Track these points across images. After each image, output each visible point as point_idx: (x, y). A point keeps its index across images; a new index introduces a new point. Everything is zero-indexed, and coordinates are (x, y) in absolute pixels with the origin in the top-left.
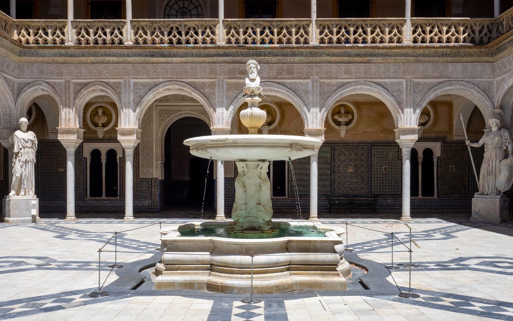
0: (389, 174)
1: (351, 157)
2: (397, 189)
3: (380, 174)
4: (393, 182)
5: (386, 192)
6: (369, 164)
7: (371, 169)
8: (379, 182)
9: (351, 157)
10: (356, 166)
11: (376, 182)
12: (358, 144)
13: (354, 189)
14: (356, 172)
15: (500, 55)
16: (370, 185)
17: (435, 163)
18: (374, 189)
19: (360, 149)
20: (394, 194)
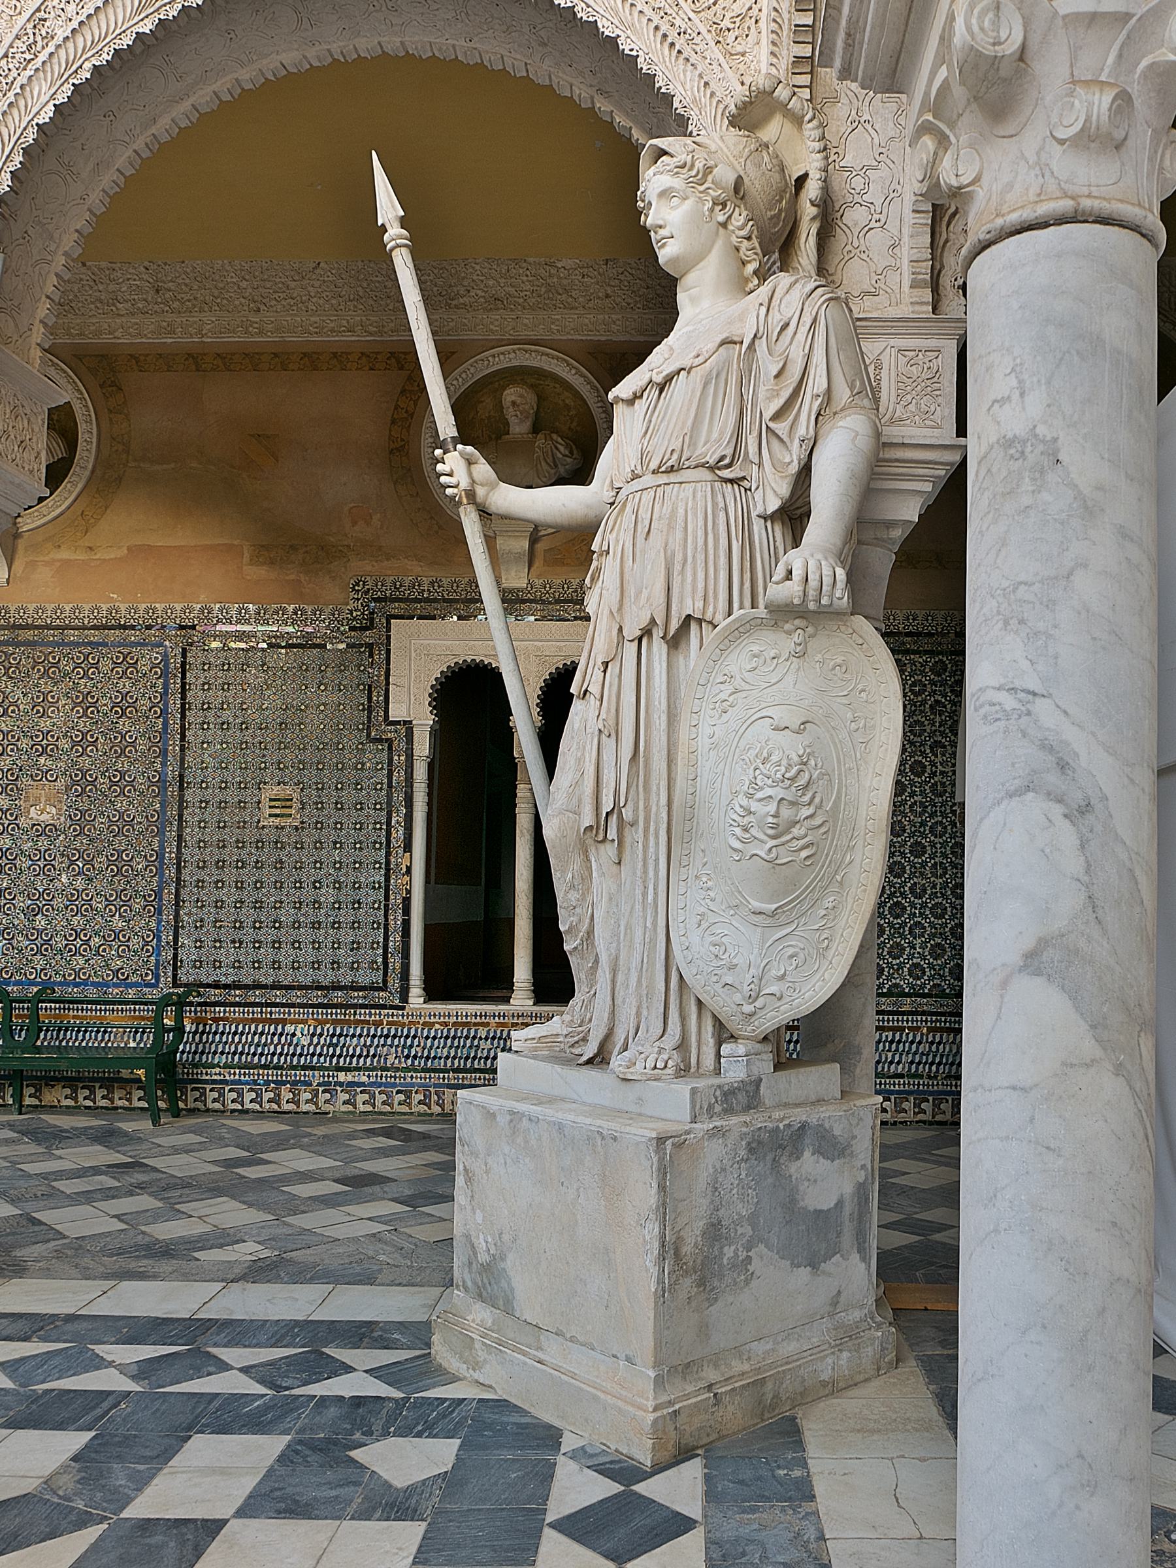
0: (299, 846)
1: (45, 724)
2: (355, 946)
3: (240, 844)
4: (327, 895)
5: (276, 965)
6: (172, 772)
7: (182, 803)
8: (229, 895)
9: (45, 724)
10: (80, 783)
11: (209, 895)
12: (95, 636)
13: (59, 942)
14: (80, 821)
16: (168, 916)
18: (199, 943)
19: (106, 665)
20: (337, 987)
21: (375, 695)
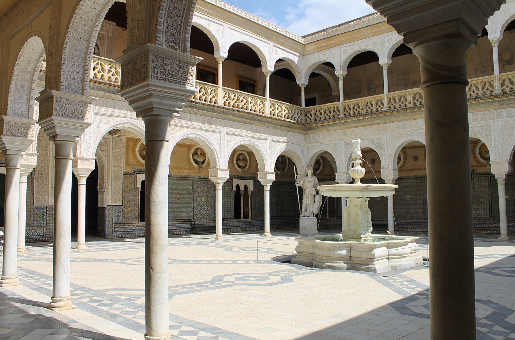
14: (207, 201)
15: (311, 131)
17: (250, 195)
21: (232, 188)
